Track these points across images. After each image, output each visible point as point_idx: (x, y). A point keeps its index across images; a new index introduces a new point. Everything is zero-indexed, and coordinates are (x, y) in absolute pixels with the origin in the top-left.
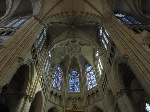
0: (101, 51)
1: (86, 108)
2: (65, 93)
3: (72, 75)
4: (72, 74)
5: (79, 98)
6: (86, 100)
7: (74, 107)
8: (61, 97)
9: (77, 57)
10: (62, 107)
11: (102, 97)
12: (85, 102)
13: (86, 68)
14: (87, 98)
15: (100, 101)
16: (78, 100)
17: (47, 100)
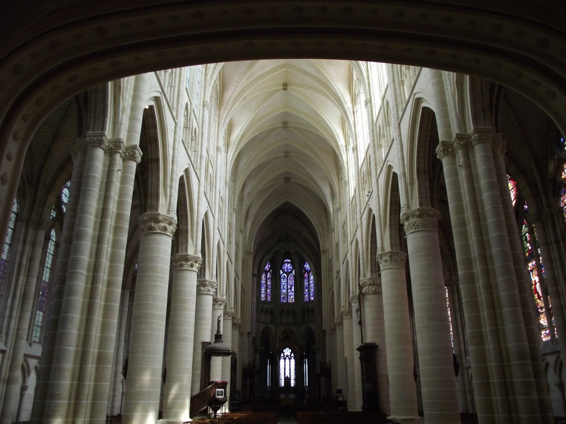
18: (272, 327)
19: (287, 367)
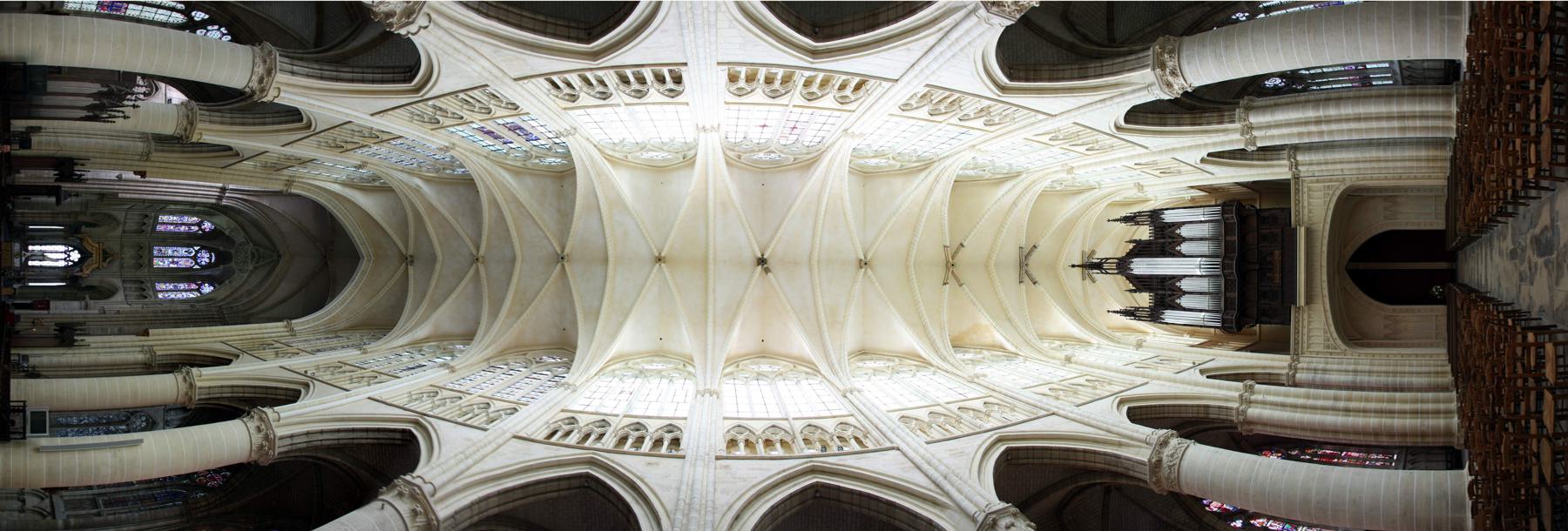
18: (118, 232)
19: (56, 255)
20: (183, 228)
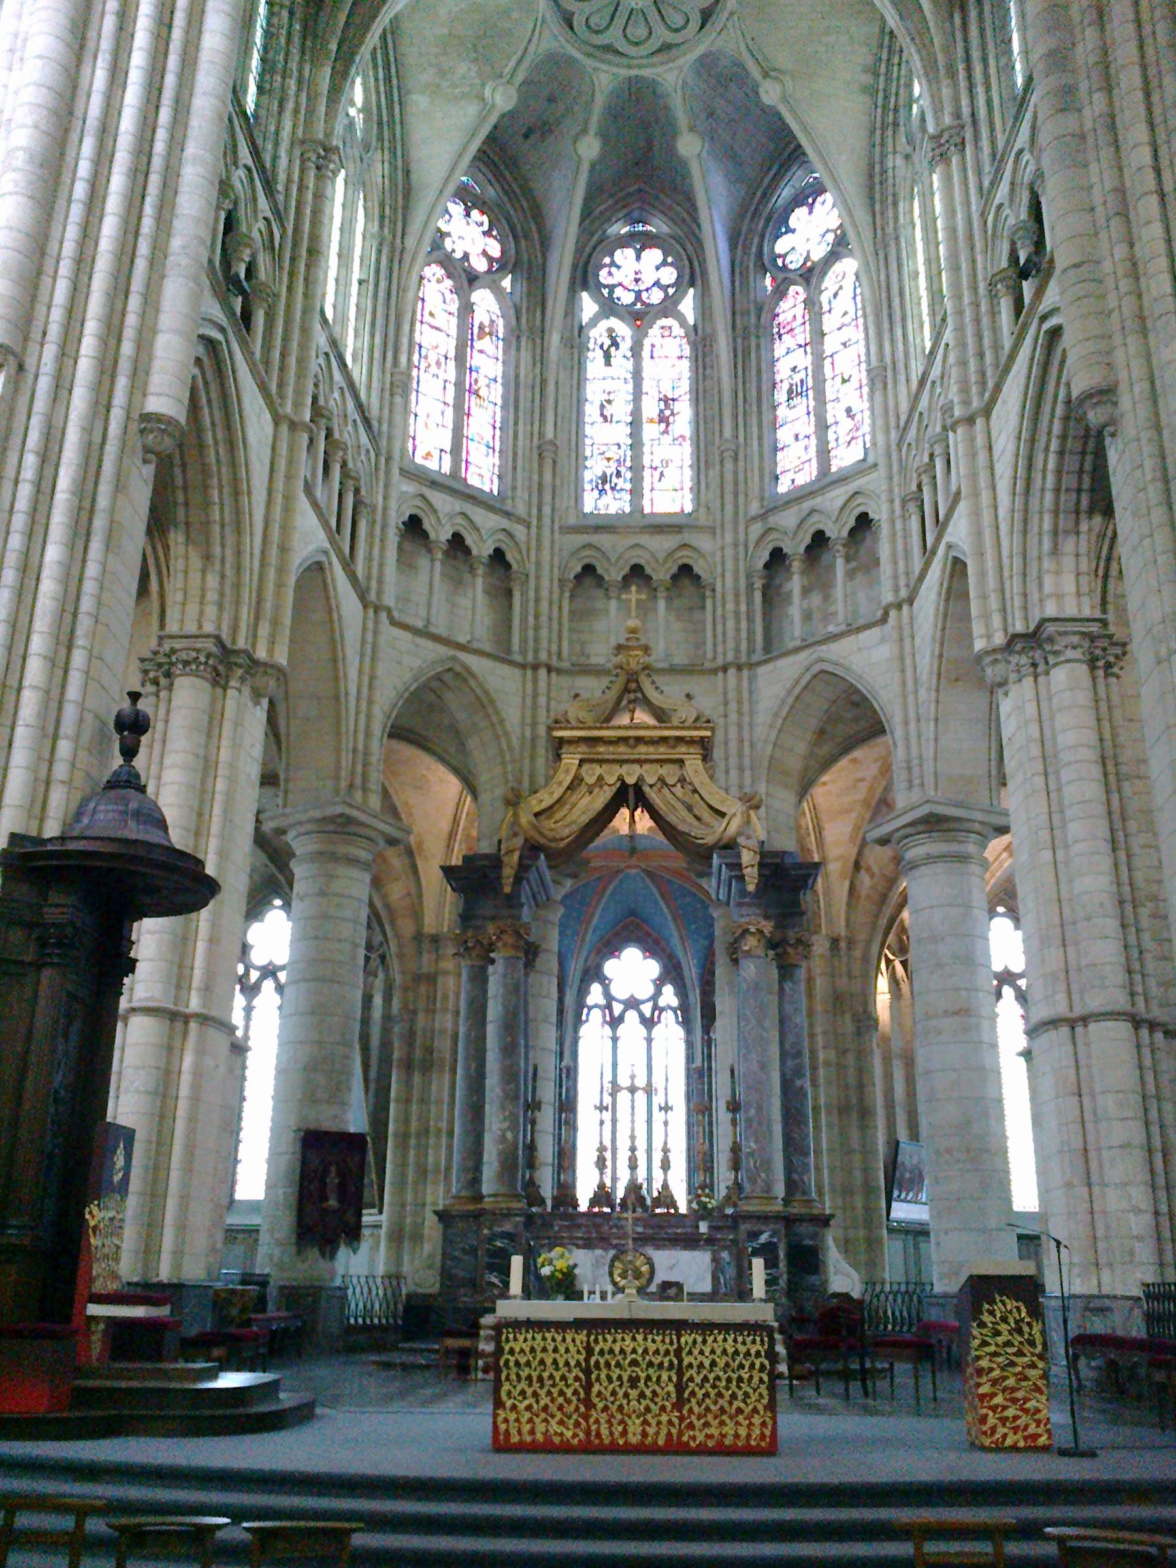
0: (956, 99)
1: (740, 680)
2: (539, 527)
3: (609, 307)
4: (612, 288)
5: (686, 570)
6: (750, 602)
7: (626, 690)
8: (508, 566)
9: (673, 77)
10: (523, 666)
11: (903, 593)
12: (738, 621)
13: (780, 223)
14: (758, 584)
15: (876, 630)
16: (669, 599)
17: (383, 615)
18: (502, 681)
20: (489, 361)
